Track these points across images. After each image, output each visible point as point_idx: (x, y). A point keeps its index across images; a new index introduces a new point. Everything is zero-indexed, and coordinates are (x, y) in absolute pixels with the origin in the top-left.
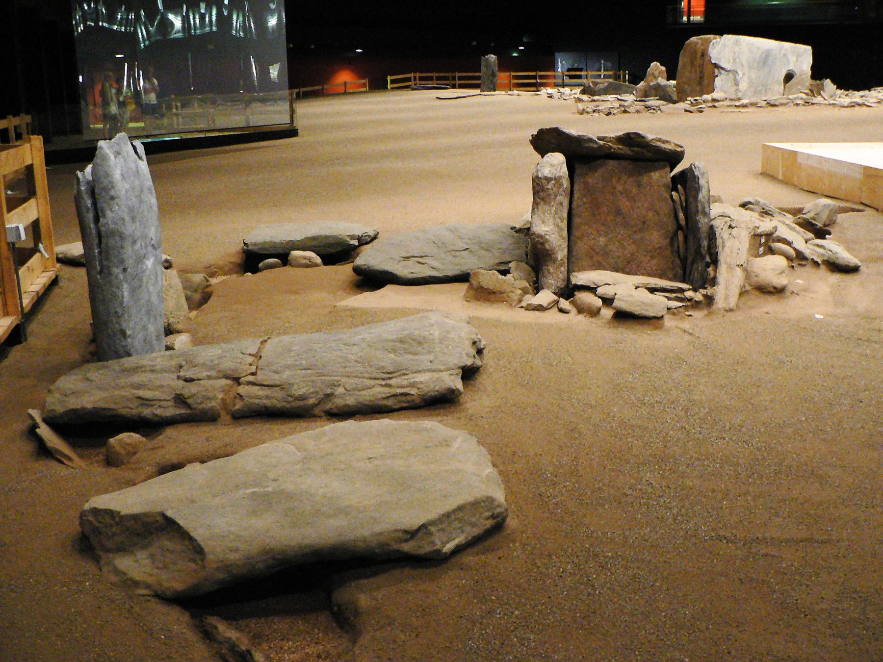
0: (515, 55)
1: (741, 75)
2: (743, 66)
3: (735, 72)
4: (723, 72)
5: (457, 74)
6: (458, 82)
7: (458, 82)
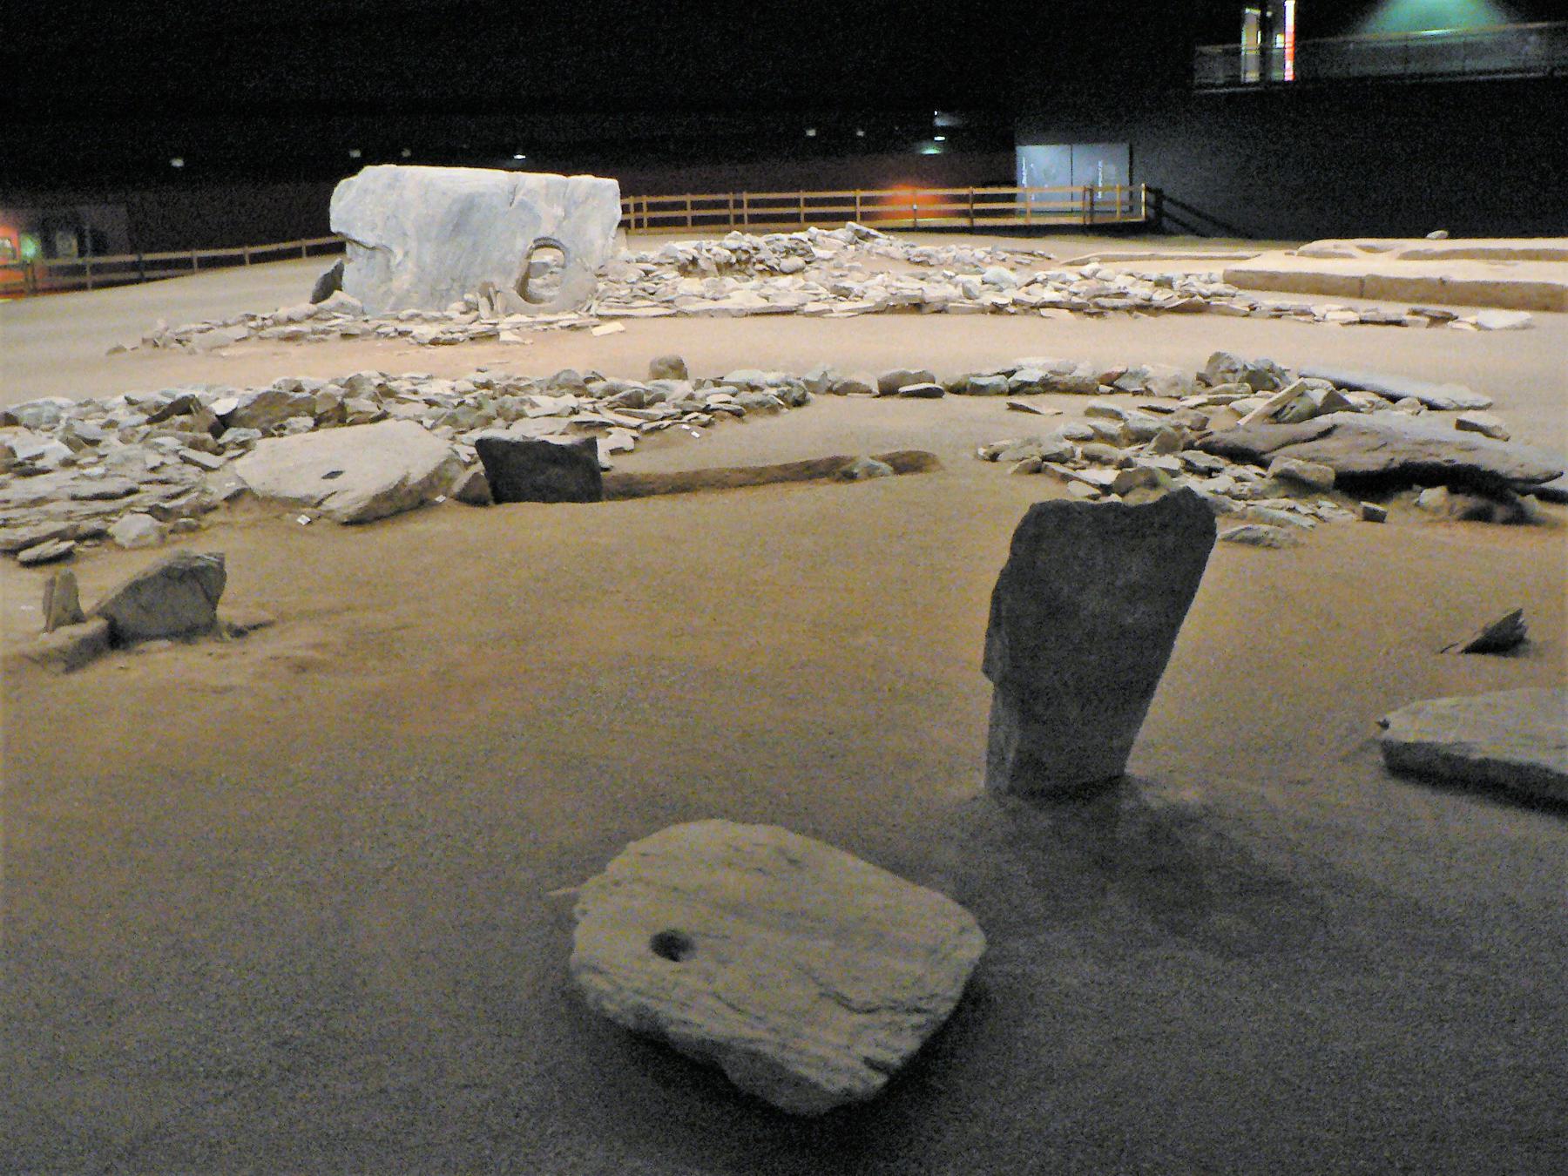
0: (931, 151)
1: (400, 256)
2: (405, 234)
3: (387, 250)
4: (361, 250)
5: (746, 197)
6: (746, 211)
7: (746, 211)
